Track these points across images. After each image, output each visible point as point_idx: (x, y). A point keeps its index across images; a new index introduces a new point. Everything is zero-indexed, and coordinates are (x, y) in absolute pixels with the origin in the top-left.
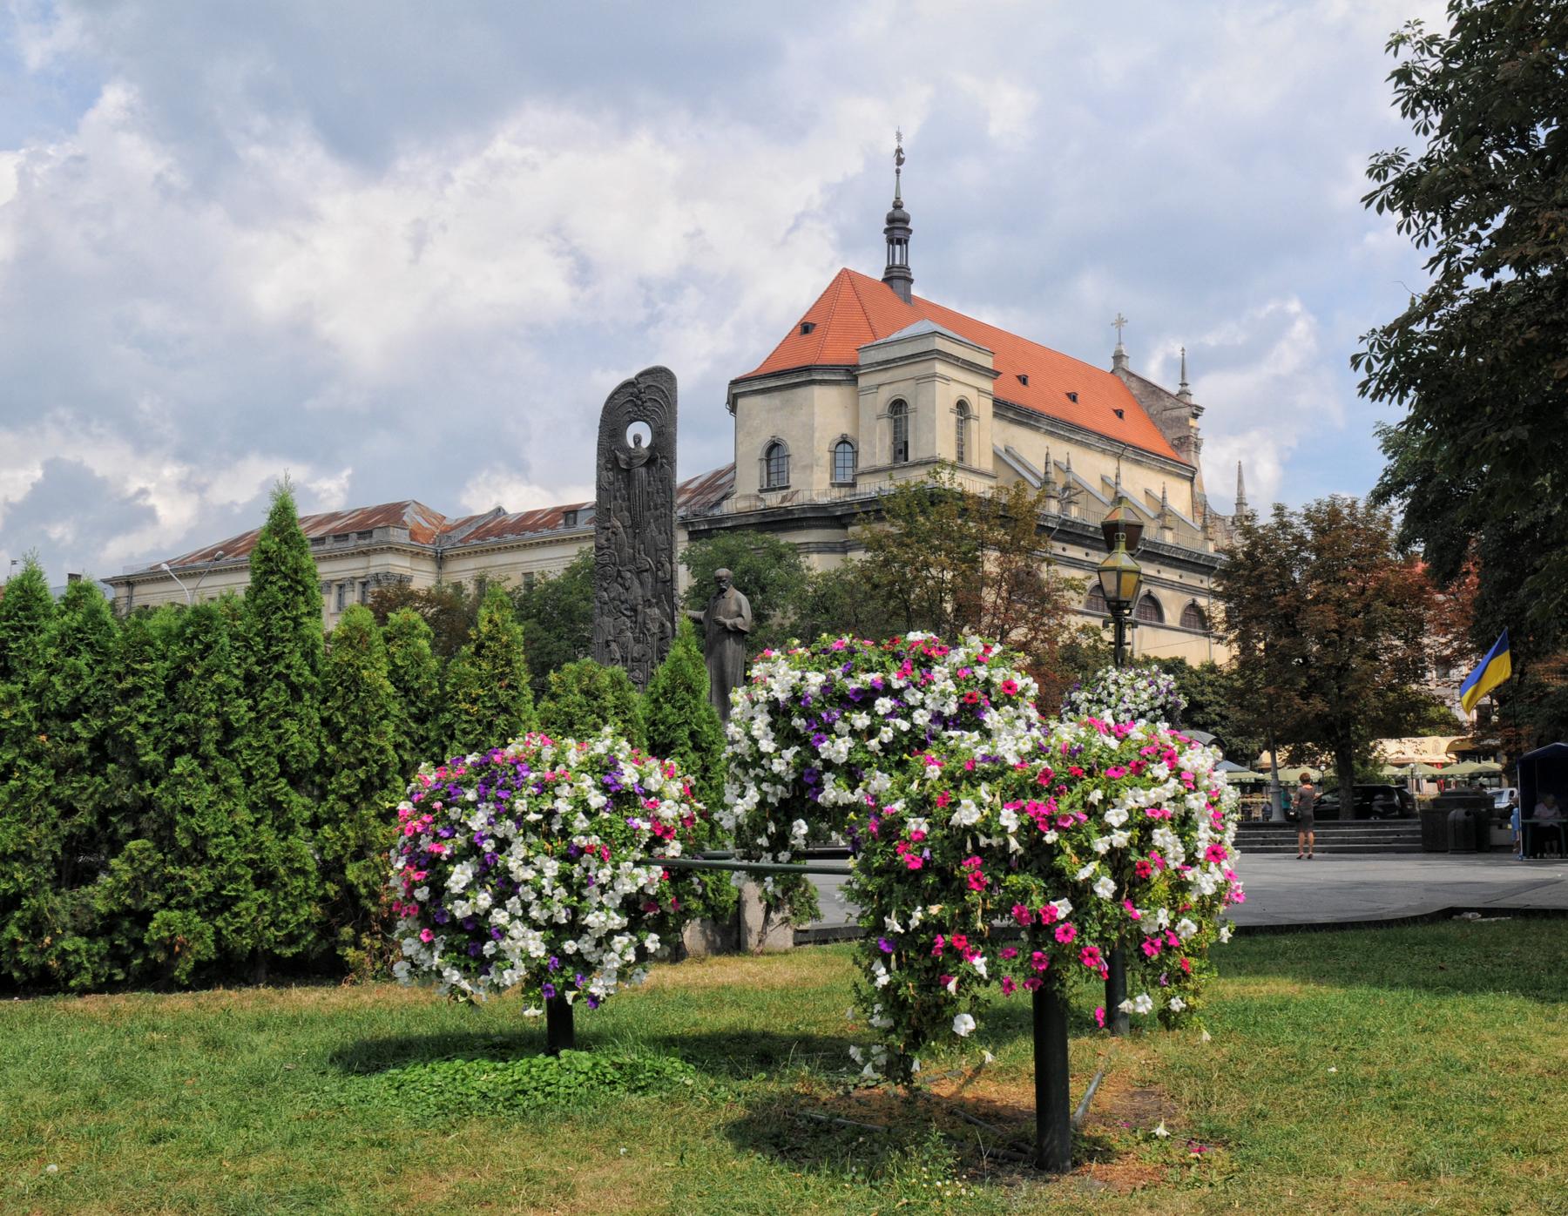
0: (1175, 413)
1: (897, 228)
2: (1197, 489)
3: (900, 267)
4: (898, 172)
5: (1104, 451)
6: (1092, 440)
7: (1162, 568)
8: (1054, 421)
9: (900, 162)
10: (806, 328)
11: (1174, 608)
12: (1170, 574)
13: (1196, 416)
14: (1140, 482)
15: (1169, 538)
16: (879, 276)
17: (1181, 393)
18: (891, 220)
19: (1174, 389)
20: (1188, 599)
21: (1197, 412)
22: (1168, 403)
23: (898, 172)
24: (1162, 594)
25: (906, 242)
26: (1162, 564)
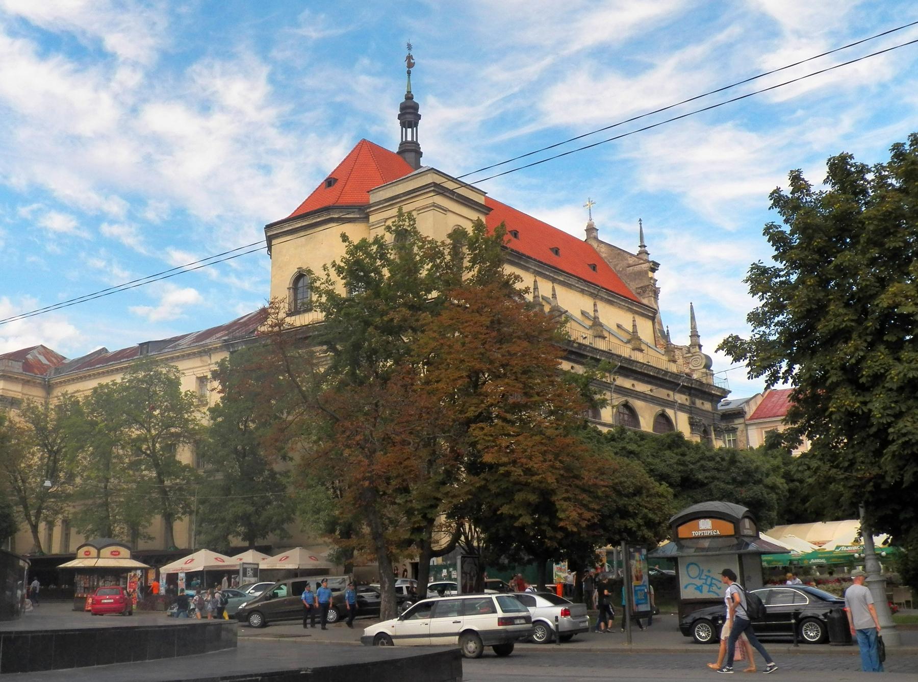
0: (637, 268)
1: (409, 115)
2: (657, 326)
3: (412, 142)
4: (409, 73)
5: (583, 291)
6: (572, 281)
7: (635, 383)
8: (541, 264)
9: (410, 65)
10: (330, 182)
11: (647, 417)
12: (642, 387)
13: (653, 270)
14: (613, 317)
15: (639, 357)
16: (395, 149)
17: (640, 253)
18: (403, 108)
19: (635, 250)
20: (658, 409)
21: (654, 267)
22: (631, 261)
23: (409, 73)
24: (638, 404)
25: (416, 125)
26: (635, 379)
